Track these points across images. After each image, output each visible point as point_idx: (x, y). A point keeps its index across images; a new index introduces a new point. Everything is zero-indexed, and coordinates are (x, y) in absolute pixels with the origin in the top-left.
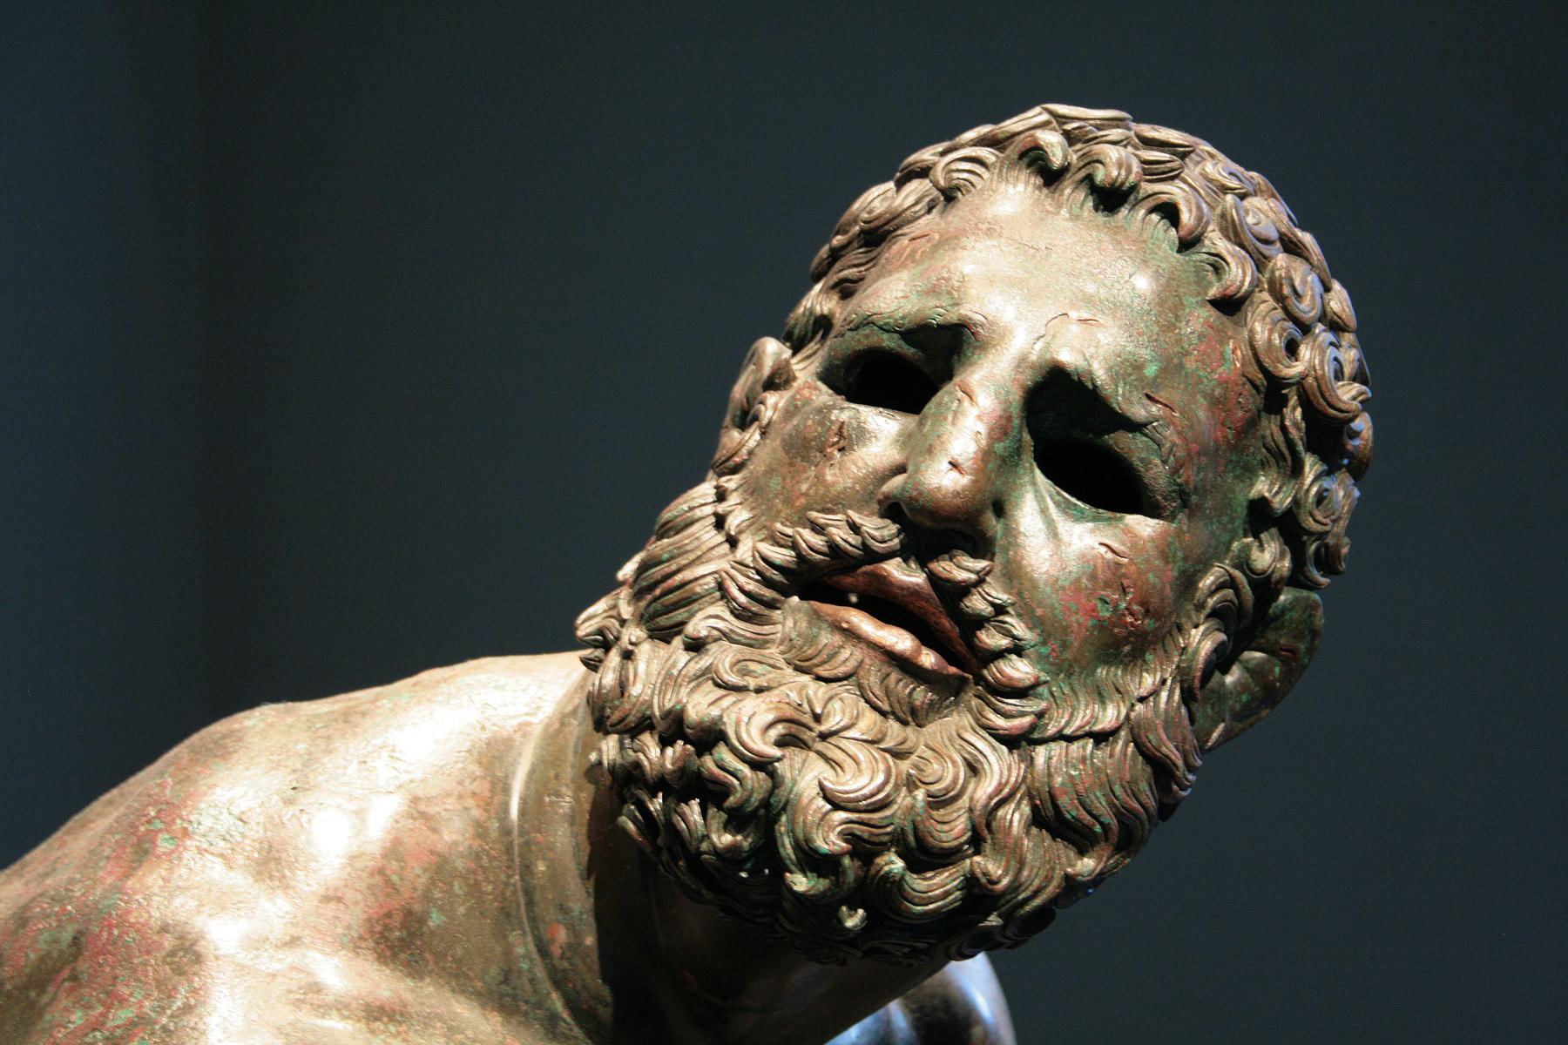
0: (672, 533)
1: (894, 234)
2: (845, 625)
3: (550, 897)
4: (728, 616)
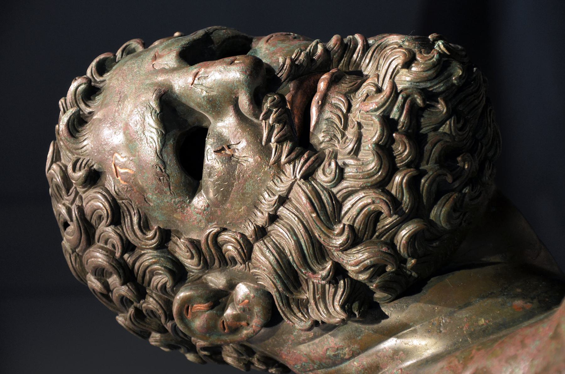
0: (283, 255)
2: (320, 102)
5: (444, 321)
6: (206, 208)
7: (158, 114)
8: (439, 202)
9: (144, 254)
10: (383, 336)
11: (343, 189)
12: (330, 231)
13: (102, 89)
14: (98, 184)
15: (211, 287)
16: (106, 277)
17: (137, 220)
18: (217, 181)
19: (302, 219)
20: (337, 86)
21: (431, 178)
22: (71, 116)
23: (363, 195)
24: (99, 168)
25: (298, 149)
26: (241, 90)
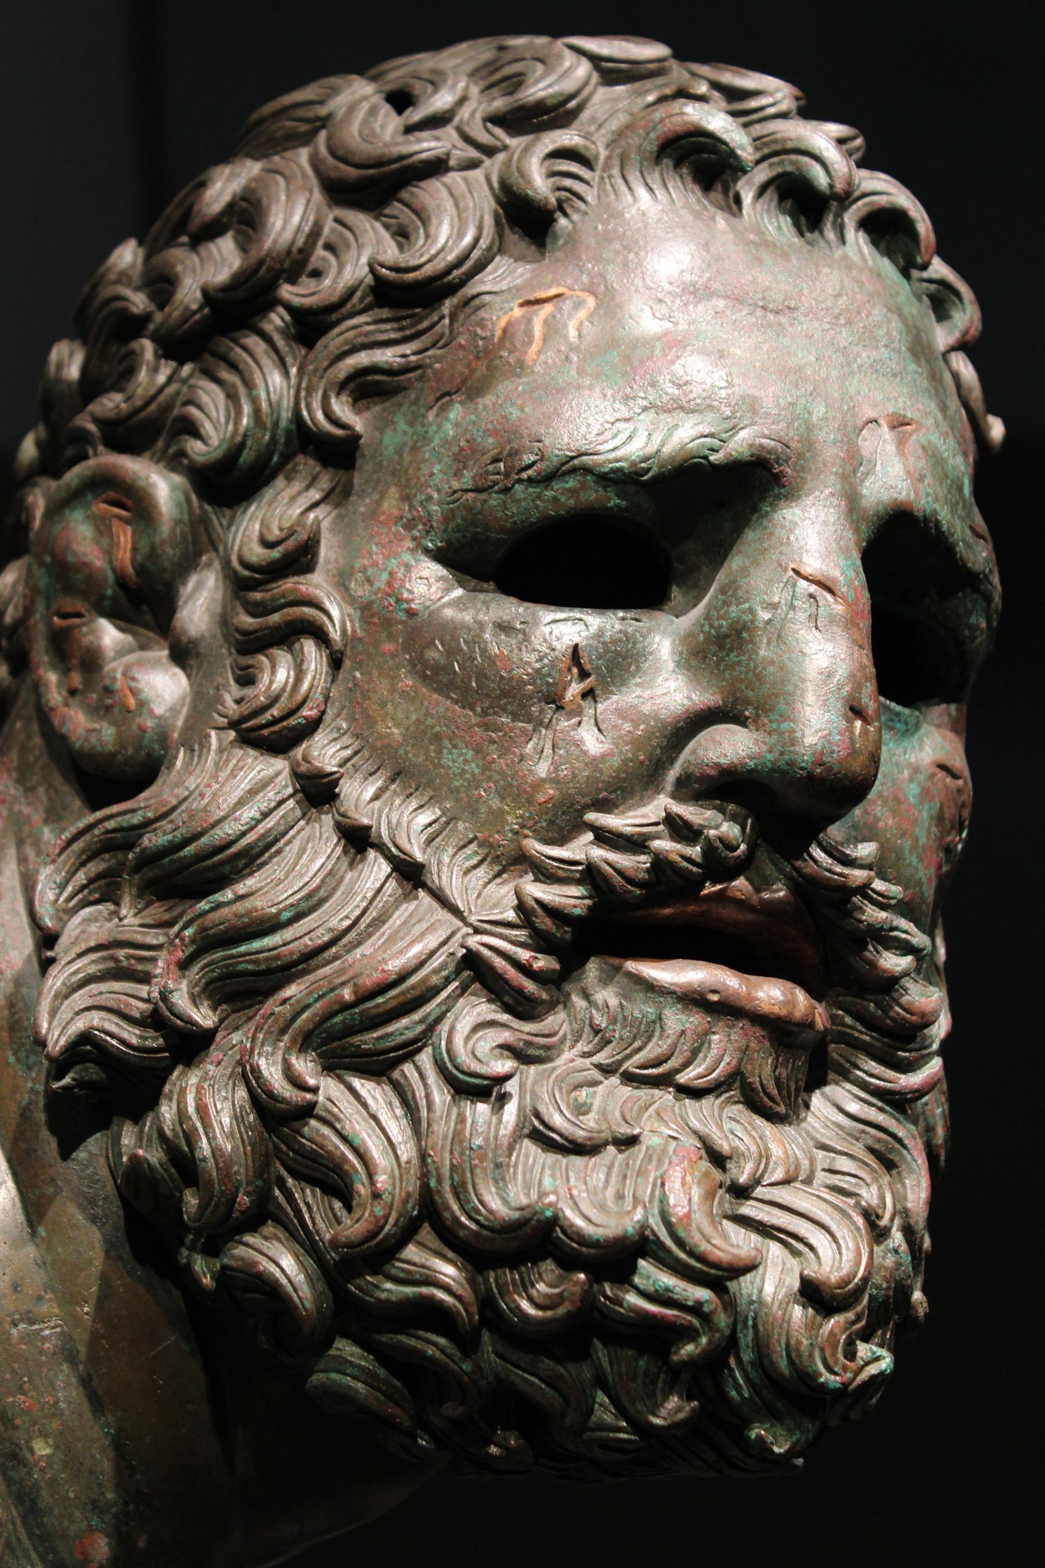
0: (241, 863)
2: (715, 998)
3: (72, 1495)
4: (505, 1017)
5: (47, 1332)
6: (405, 606)
7: (706, 458)
8: (382, 1372)
9: (286, 374)
10: (11, 1135)
11: (425, 1085)
12: (300, 1041)
13: (816, 235)
14: (507, 230)
15: (184, 583)
16: (238, 232)
17: (387, 362)
18: (484, 651)
19: (345, 941)
20: (768, 1044)
21: (452, 1365)
22: (725, 143)
23: (404, 1158)
24: (556, 238)
25: (566, 933)
26: (764, 743)
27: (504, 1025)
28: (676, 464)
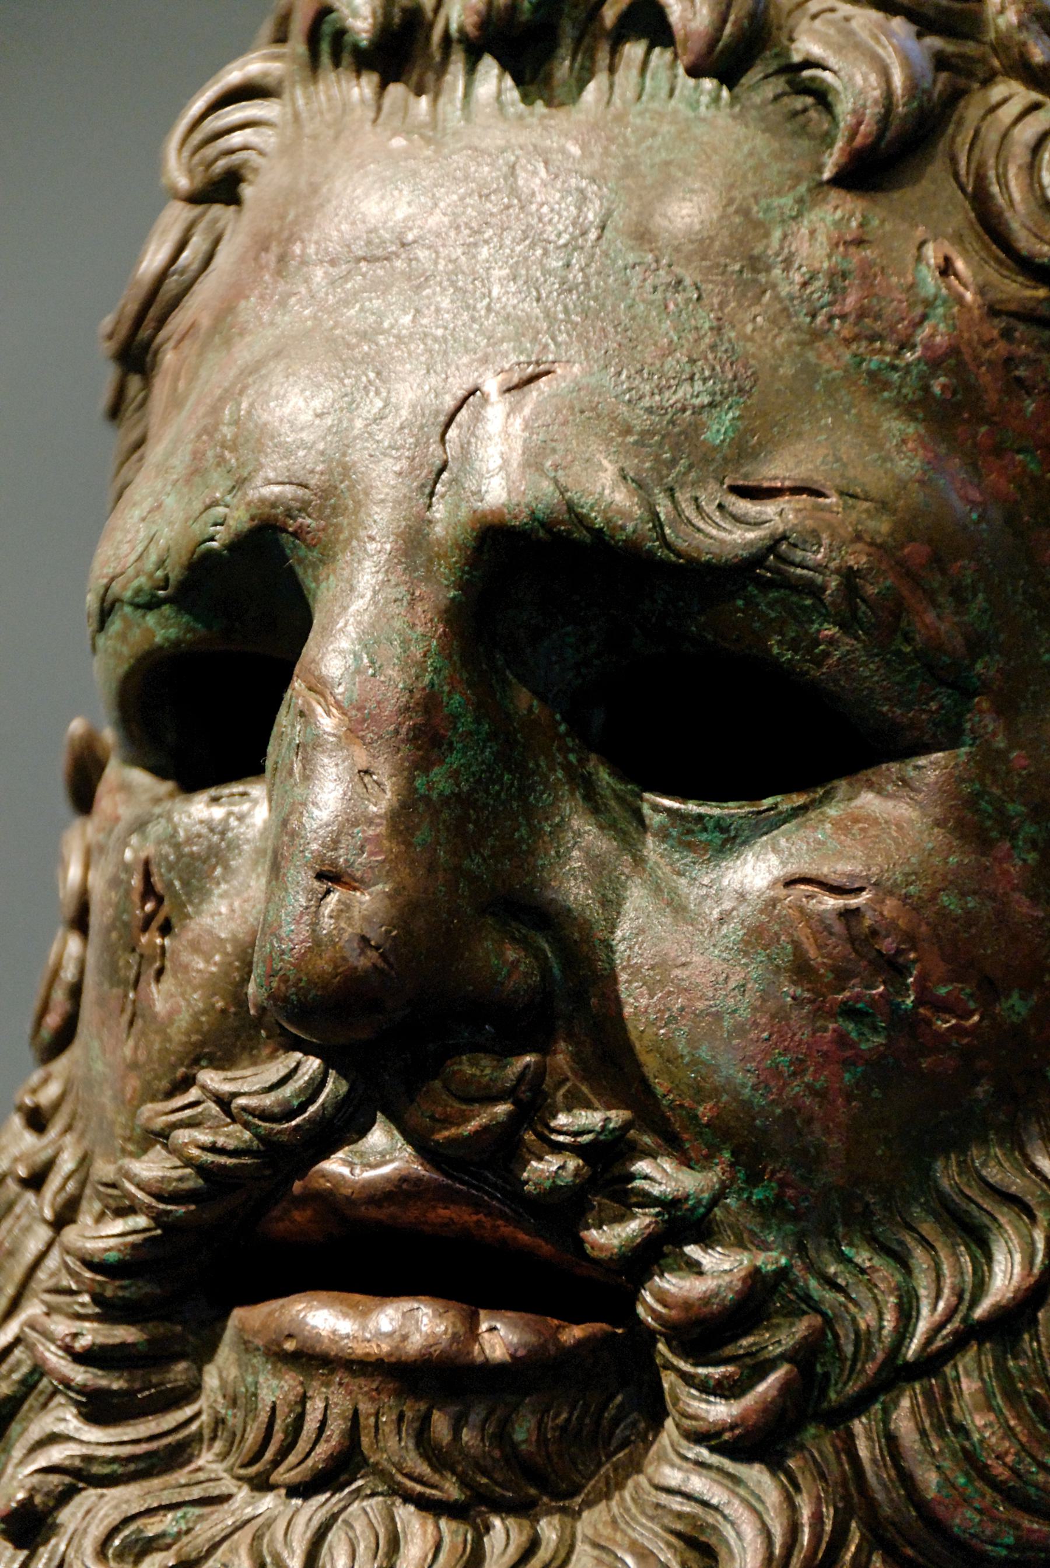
1: (154, 345)
2: (290, 1346)
27: (67, 1438)
28: (184, 559)
